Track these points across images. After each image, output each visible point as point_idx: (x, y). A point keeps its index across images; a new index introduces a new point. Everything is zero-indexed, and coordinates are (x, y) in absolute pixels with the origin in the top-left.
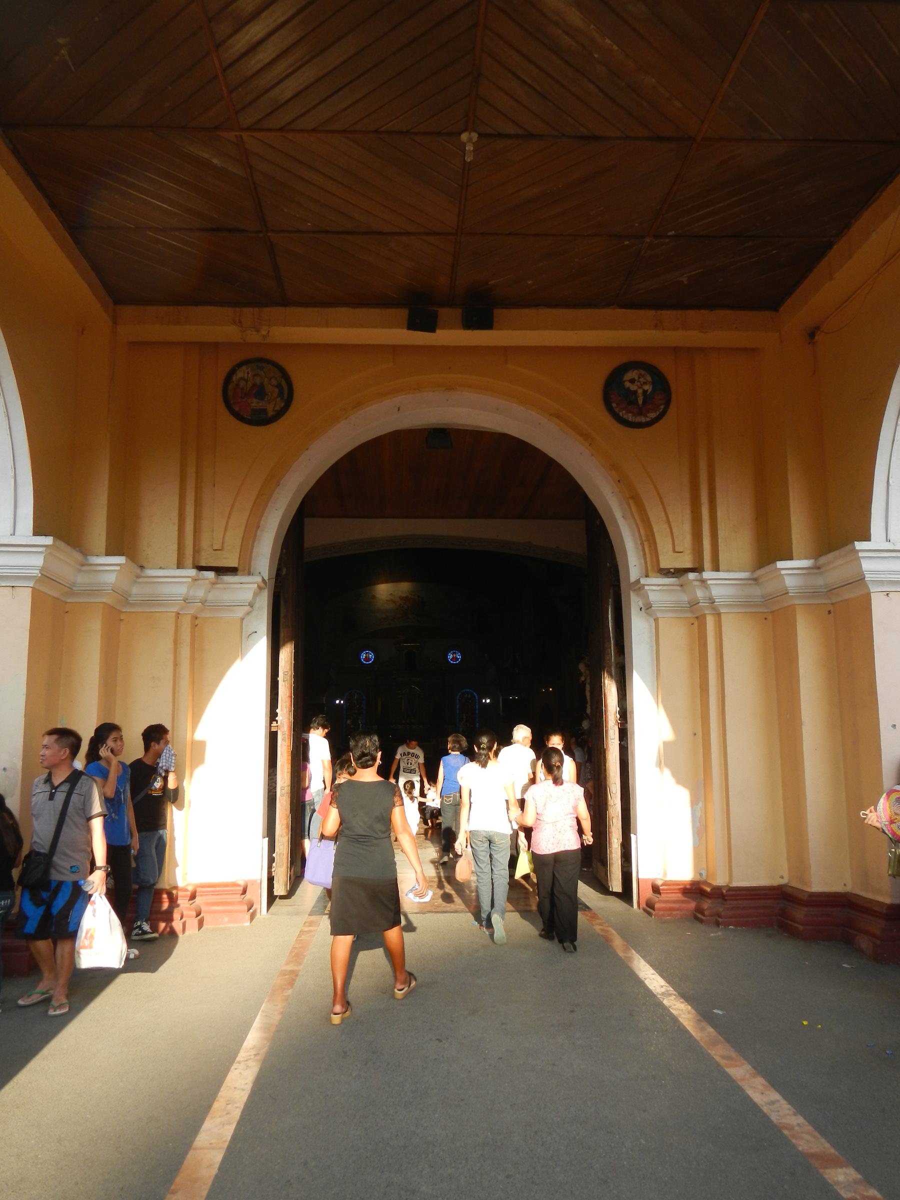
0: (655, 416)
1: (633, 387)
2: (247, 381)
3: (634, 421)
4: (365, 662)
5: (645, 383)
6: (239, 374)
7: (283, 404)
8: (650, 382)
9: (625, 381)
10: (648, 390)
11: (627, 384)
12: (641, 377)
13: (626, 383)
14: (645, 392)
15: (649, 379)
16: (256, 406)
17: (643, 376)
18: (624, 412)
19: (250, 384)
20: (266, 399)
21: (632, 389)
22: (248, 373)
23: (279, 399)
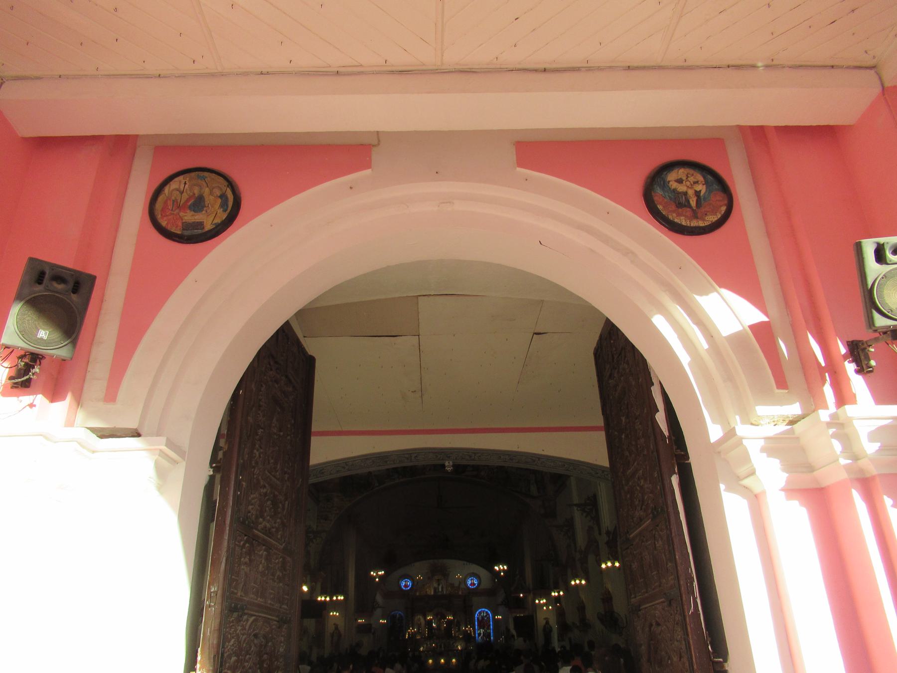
0: (716, 219)
1: (681, 188)
2: (182, 193)
3: (689, 225)
4: (404, 588)
5: (696, 182)
6: (174, 185)
7: (224, 216)
8: (702, 182)
9: (669, 181)
10: (700, 191)
11: (674, 185)
12: (689, 176)
13: (671, 183)
14: (697, 193)
15: (700, 178)
16: (191, 220)
17: (693, 175)
18: (674, 215)
19: (185, 196)
20: (204, 212)
21: (680, 191)
22: (185, 184)
23: (222, 209)
